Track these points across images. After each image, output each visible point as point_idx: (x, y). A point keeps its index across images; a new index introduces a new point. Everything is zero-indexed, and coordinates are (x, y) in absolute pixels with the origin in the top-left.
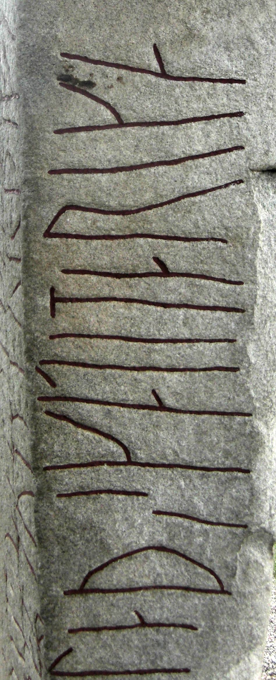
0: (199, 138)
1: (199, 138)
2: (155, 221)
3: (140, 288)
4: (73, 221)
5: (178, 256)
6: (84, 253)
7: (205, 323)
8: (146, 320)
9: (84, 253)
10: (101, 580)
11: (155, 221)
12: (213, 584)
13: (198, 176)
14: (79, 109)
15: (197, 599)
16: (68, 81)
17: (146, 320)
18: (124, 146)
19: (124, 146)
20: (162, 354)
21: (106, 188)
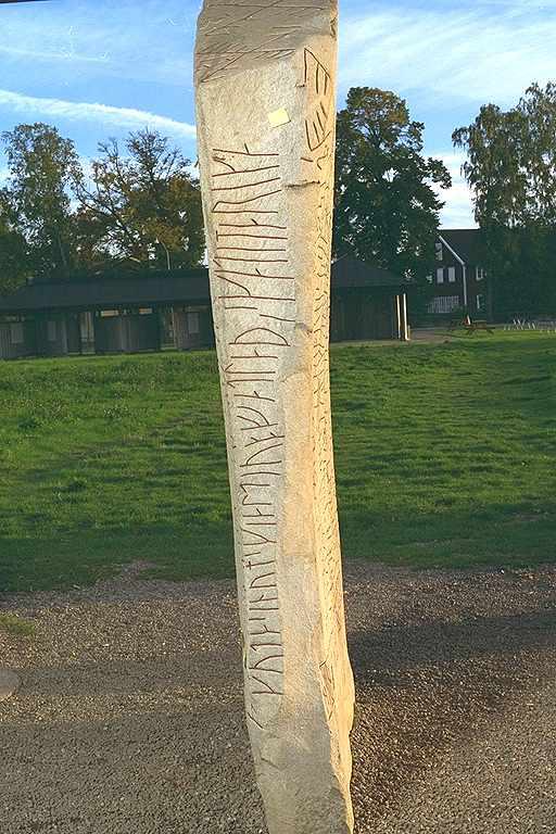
0: (264, 175)
1: (264, 175)
2: (252, 205)
3: (247, 231)
4: (221, 207)
5: (261, 219)
6: (229, 218)
7: (270, 244)
8: (250, 243)
9: (229, 218)
10: (243, 339)
11: (252, 205)
12: (283, 342)
13: (259, 190)
14: (219, 168)
15: (277, 348)
16: (216, 159)
17: (250, 243)
18: (234, 180)
19: (234, 180)
20: (256, 255)
21: (229, 195)
